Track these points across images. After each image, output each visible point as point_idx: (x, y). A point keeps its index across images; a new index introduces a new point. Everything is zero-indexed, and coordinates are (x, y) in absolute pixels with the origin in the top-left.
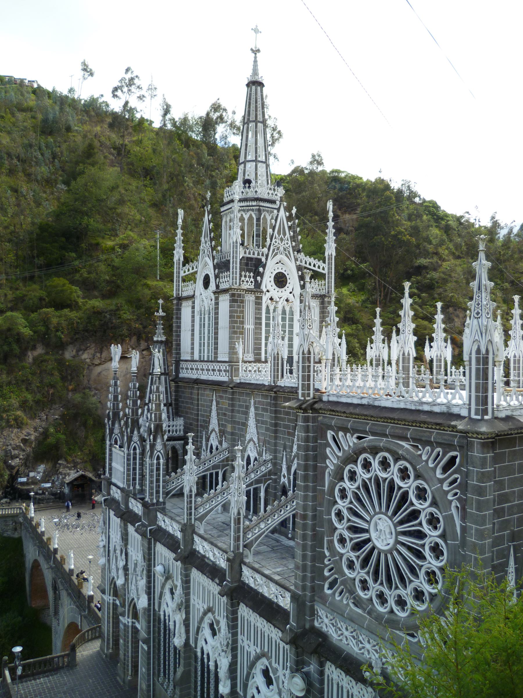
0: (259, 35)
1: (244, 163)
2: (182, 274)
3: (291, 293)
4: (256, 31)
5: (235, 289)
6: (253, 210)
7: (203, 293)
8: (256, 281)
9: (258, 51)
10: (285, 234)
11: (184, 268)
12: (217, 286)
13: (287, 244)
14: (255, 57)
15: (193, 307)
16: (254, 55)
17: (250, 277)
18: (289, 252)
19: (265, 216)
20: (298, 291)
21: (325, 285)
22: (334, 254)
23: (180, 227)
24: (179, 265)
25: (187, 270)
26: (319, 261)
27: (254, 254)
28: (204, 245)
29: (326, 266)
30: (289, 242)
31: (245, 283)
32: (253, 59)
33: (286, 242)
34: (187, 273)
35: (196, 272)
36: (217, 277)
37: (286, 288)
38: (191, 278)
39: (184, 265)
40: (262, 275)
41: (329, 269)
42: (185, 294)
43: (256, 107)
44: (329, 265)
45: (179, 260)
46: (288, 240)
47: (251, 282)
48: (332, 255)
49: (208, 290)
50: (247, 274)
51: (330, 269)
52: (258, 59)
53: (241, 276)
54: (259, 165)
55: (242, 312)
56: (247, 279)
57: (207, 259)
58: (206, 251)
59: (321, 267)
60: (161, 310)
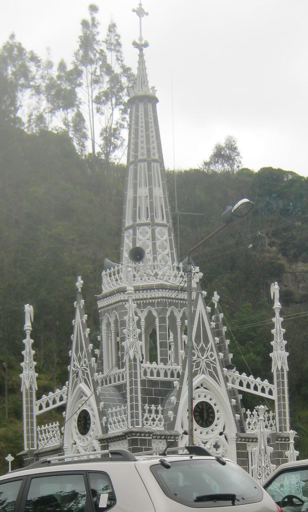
0: (145, 18)
1: (134, 227)
2: (37, 412)
3: (221, 434)
4: (140, 12)
5: (137, 433)
6: (152, 304)
7: (78, 441)
8: (167, 419)
9: (146, 45)
10: (206, 341)
11: (40, 401)
12: (105, 430)
13: (212, 356)
14: (141, 56)
16: (137, 51)
17: (157, 412)
18: (215, 369)
19: (172, 313)
20: (232, 431)
21: (274, 418)
22: (286, 368)
23: (28, 333)
24: (31, 396)
25: (44, 405)
26: (262, 380)
27: (158, 375)
28: (77, 364)
29: (274, 388)
30: (215, 354)
31: (150, 422)
32: (137, 58)
33: (209, 353)
34: (45, 409)
35: (63, 408)
36: (102, 414)
37: (213, 426)
39: (39, 397)
41: (279, 393)
43: (147, 136)
44: (278, 386)
45: (31, 388)
46: (212, 350)
47: (160, 420)
48: (282, 370)
49: (87, 436)
50: (153, 407)
52: (145, 58)
53: (144, 410)
54: (158, 229)
56: (153, 415)
57: (82, 386)
58: (80, 374)
59: (267, 390)
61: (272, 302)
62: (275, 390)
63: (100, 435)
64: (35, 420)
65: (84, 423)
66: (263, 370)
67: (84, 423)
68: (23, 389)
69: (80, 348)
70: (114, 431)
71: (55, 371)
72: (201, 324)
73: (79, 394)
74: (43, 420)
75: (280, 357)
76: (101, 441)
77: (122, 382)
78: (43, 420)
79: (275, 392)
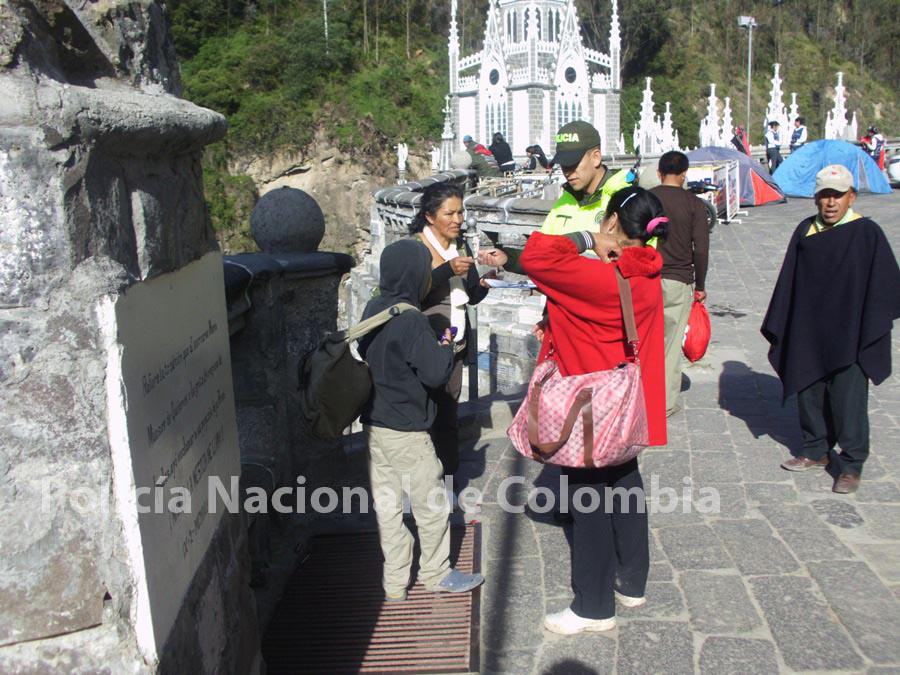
2: (458, 69)
8: (549, 76)
10: (573, 29)
15: (477, 103)
23: (454, 18)
28: (490, 39)
29: (611, 60)
36: (508, 72)
38: (474, 71)
39: (460, 59)
40: (554, 71)
42: (462, 91)
51: (615, 62)
55: (541, 107)
58: (493, 46)
60: (447, 108)
61: (612, 6)
62: (613, 60)
63: (507, 85)
64: (457, 74)
65: (494, 77)
66: (604, 49)
67: (494, 77)
68: (450, 54)
69: (493, 29)
70: (516, 83)
71: (473, 41)
72: (571, 19)
73: (485, 60)
74: (462, 74)
75: (615, 41)
76: (508, 90)
77: (524, 51)
78: (462, 74)
79: (611, 63)
